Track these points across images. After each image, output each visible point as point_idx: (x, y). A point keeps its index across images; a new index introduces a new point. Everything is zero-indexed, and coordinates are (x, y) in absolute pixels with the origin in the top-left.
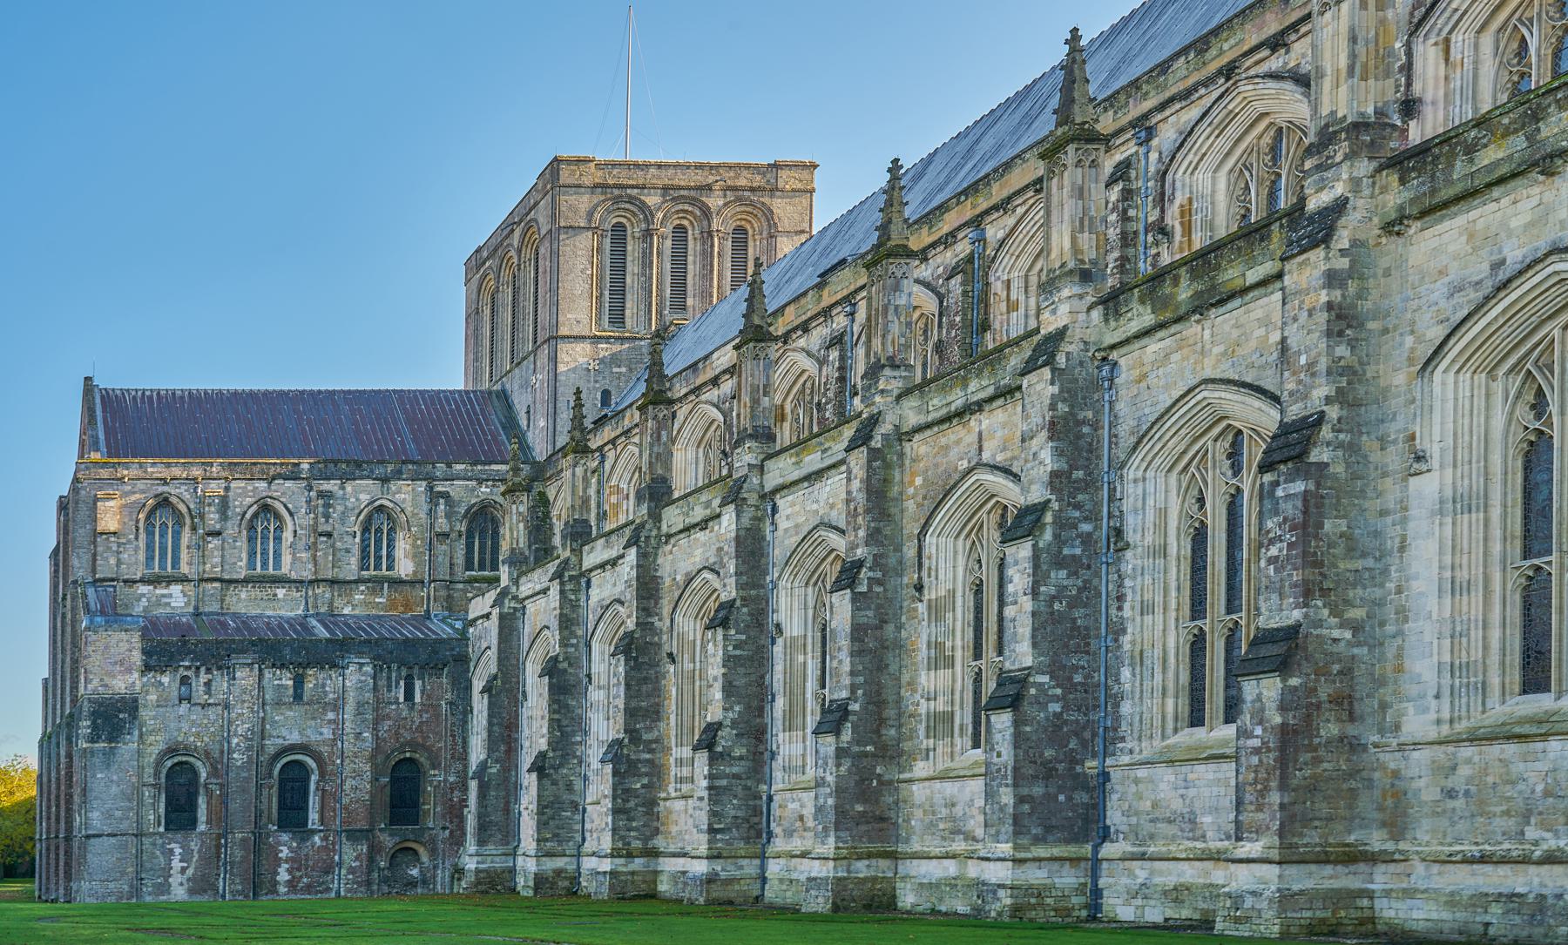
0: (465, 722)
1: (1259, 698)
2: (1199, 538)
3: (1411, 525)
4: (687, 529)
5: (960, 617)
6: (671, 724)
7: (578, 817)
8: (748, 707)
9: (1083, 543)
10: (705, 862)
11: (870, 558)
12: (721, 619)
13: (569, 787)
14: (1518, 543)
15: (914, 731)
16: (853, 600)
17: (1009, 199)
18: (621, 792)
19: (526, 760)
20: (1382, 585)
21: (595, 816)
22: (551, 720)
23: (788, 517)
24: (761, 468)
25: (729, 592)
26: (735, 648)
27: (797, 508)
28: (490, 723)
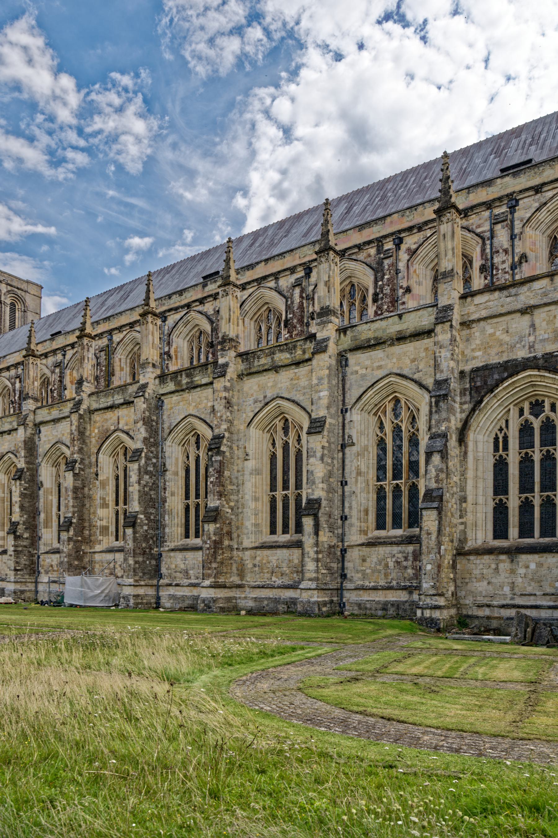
1: (208, 531)
2: (187, 471)
3: (245, 476)
8: (29, 516)
9: (154, 466)
10: (13, 584)
11: (79, 459)
12: (19, 475)
14: (269, 487)
15: (95, 532)
20: (238, 495)
24: (34, 412)
25: (21, 464)
26: (24, 489)
27: (49, 433)
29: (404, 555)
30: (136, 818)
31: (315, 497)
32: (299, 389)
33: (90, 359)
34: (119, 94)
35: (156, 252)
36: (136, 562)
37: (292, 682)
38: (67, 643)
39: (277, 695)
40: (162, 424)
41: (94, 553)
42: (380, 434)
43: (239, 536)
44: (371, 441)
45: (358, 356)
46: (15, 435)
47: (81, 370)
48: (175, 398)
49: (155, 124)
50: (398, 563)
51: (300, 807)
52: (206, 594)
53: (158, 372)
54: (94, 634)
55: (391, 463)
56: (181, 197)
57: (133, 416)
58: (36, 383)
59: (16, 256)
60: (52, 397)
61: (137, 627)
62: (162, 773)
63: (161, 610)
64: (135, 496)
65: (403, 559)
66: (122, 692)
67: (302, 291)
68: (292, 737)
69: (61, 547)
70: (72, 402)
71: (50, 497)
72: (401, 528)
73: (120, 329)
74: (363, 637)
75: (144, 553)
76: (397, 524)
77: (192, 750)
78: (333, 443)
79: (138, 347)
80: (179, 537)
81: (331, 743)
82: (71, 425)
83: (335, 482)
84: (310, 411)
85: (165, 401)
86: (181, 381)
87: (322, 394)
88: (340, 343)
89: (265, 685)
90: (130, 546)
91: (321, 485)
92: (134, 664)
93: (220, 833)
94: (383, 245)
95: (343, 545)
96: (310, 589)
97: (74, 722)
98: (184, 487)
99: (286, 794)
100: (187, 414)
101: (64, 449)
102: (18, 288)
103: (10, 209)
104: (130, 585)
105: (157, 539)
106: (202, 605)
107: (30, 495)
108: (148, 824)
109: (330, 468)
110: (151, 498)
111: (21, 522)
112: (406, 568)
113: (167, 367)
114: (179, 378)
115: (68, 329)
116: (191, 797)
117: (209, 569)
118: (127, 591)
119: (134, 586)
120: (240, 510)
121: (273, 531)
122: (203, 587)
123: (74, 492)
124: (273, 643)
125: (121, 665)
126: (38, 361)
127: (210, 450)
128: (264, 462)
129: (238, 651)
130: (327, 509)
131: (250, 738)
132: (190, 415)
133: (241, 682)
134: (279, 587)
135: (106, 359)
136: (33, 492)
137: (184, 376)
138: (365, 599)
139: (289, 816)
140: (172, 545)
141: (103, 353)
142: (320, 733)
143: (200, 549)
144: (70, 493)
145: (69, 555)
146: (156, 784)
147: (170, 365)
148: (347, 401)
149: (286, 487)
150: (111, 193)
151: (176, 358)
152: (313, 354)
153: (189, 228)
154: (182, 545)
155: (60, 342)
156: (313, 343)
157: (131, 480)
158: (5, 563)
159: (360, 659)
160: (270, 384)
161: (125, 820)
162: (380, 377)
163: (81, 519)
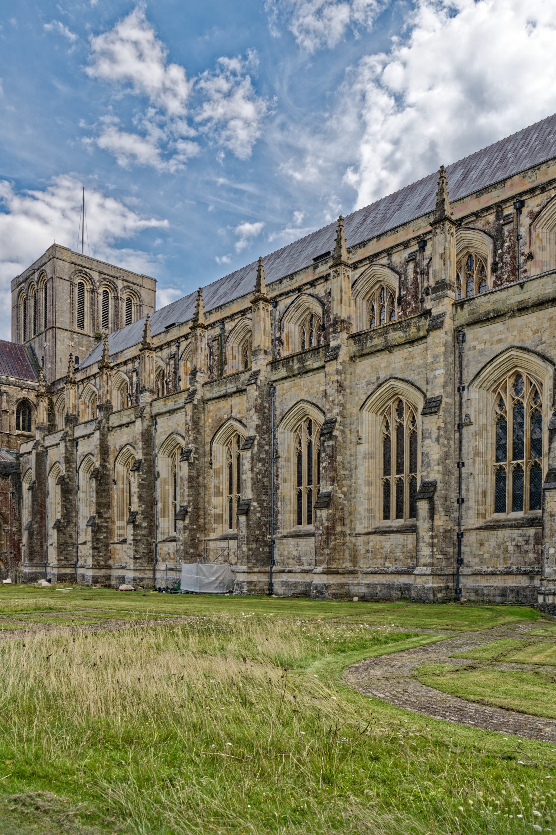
0: (19, 503)
1: (321, 516)
3: (358, 461)
4: (120, 426)
5: (225, 476)
6: (114, 512)
7: (75, 550)
8: (147, 506)
12: (137, 467)
13: (71, 536)
16: (189, 466)
17: (233, 315)
18: (95, 540)
19: (51, 523)
20: (350, 480)
21: (82, 550)
22: (62, 505)
23: (161, 427)
24: (151, 404)
25: (139, 455)
26: (142, 480)
27: (165, 424)
28: (33, 504)
29: (525, 538)
30: (251, 800)
31: (430, 479)
32: (413, 368)
33: (203, 349)
34: (227, 79)
35: (267, 237)
36: (249, 549)
37: (406, 669)
38: (184, 629)
39: (391, 682)
40: (275, 411)
41: (209, 540)
42: (499, 412)
43: (351, 522)
44: (490, 420)
45: (476, 330)
46: (133, 427)
47: (194, 360)
48: (287, 384)
49: (263, 105)
50: (518, 546)
51: (414, 795)
52: (319, 580)
53: (270, 358)
54: (209, 620)
55: (511, 442)
56: (291, 178)
57: (245, 404)
58: (152, 376)
59: (131, 251)
60: (168, 389)
61: (251, 613)
62: (276, 756)
63: (274, 596)
64: (249, 484)
65: (523, 543)
66: (238, 677)
67: (416, 266)
68: (406, 725)
69: (177, 536)
70: (186, 392)
71: (167, 487)
72: (522, 510)
73: (231, 317)
74: (480, 624)
75: (257, 540)
76: (517, 505)
77: (306, 735)
78: (449, 423)
79: (249, 334)
80: (292, 524)
81: (446, 732)
82: (186, 415)
83: (451, 463)
84: (425, 391)
85: (277, 387)
86: (292, 366)
87: (437, 372)
88: (456, 318)
89: (378, 672)
90: (244, 533)
91: (436, 468)
92: (248, 650)
93: (334, 818)
94: (502, 210)
95: (460, 529)
96: (425, 575)
97: (191, 705)
98: (296, 473)
99: (401, 782)
100: (299, 399)
101: (179, 439)
102: (133, 284)
103: (125, 205)
104: (244, 572)
105: (270, 526)
106: (315, 591)
107: (148, 485)
108: (262, 806)
109: (446, 449)
110: (264, 486)
111: (140, 512)
112: (527, 552)
113: (279, 353)
114: (291, 364)
115: (182, 320)
116: (305, 782)
117: (322, 555)
118: (241, 578)
119: (247, 572)
120: (353, 495)
121: (387, 516)
122: (315, 573)
123: (189, 482)
124: (386, 630)
125: (235, 650)
126: (154, 354)
127: (322, 435)
128: (377, 445)
129: (351, 637)
130: (443, 492)
131: (364, 724)
132: (302, 400)
133: (354, 669)
134: (392, 573)
135: (218, 348)
136: (150, 483)
137: (295, 361)
138: (483, 585)
139: (403, 805)
140: (285, 532)
141: (215, 343)
142: (435, 721)
143: (313, 535)
144: (186, 483)
145: (185, 543)
146: (271, 767)
147: (281, 351)
148: (464, 378)
149: (400, 470)
150: (221, 180)
151: (288, 344)
152: (428, 331)
153: (299, 210)
154: (295, 532)
155: (174, 334)
156: (428, 319)
157: (244, 468)
158: (125, 552)
159: (477, 646)
160: (383, 365)
161: (240, 801)
162: (500, 351)
163: (196, 508)
